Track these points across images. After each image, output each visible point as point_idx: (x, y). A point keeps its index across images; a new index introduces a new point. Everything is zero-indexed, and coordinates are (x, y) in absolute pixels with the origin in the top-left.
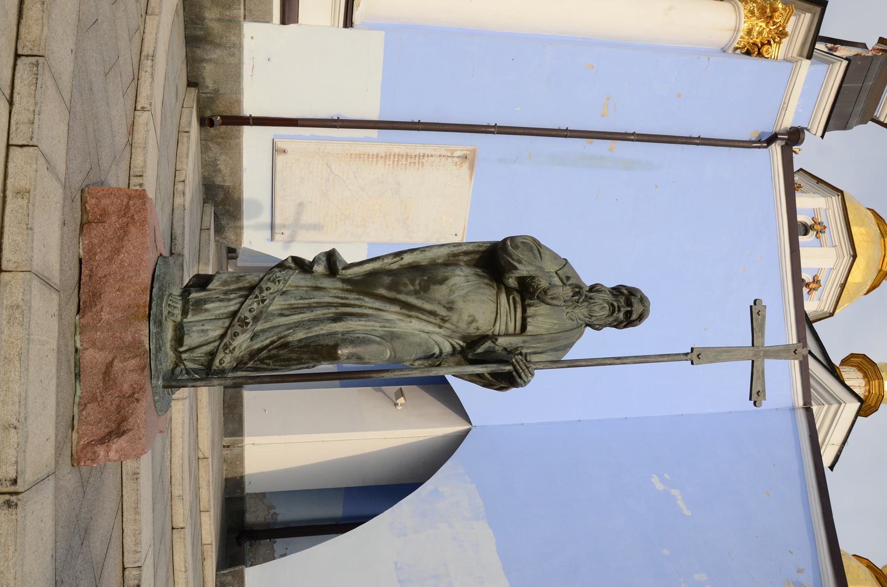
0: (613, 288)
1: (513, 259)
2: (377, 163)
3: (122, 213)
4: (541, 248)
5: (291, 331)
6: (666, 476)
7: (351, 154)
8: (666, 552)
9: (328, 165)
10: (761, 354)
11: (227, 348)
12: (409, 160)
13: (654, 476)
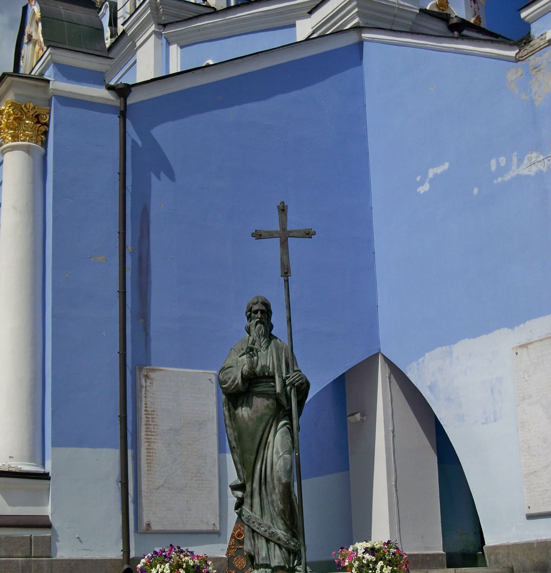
0: (248, 320)
1: (232, 385)
2: (154, 449)
4: (225, 367)
5: (276, 508)
6: (418, 179)
7: (148, 470)
8: (476, 191)
9: (157, 489)
11: (286, 542)
12: (150, 423)
13: (418, 190)
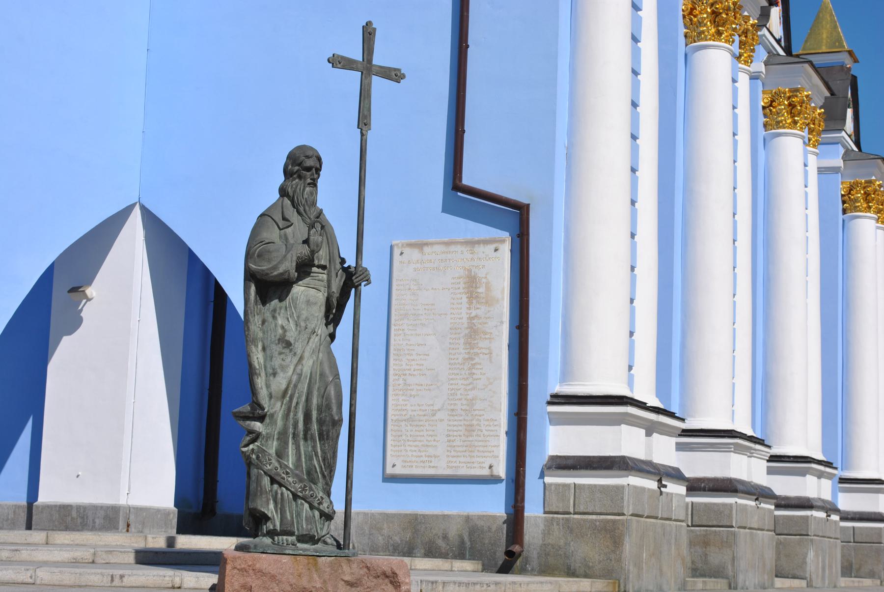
3: (245, 573)
10: (368, 65)
